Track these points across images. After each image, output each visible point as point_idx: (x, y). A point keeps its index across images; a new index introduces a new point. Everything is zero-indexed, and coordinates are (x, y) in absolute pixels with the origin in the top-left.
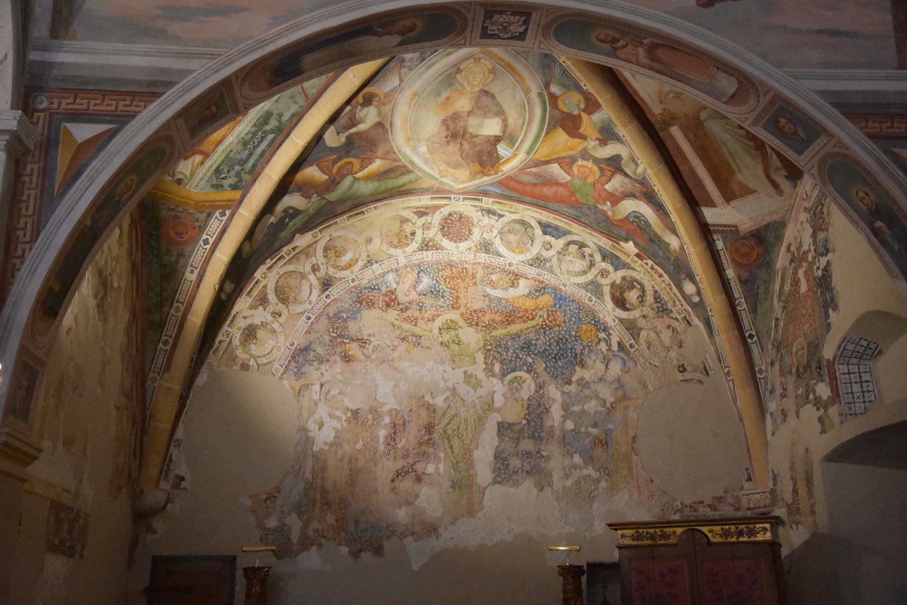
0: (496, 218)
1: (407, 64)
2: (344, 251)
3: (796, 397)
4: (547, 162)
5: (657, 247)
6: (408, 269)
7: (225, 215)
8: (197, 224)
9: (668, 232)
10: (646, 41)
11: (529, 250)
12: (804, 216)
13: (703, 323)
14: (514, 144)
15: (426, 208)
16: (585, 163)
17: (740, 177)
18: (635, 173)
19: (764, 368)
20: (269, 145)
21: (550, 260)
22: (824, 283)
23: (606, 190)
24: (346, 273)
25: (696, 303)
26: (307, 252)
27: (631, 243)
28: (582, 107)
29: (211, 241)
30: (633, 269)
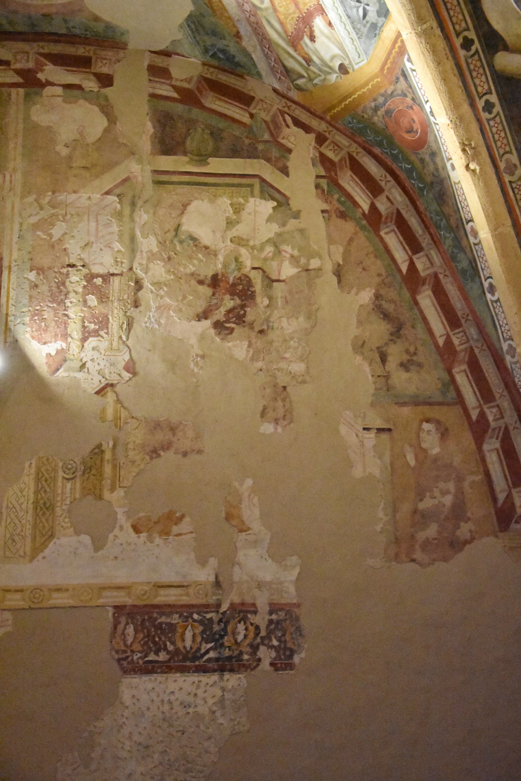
8: (409, 100)
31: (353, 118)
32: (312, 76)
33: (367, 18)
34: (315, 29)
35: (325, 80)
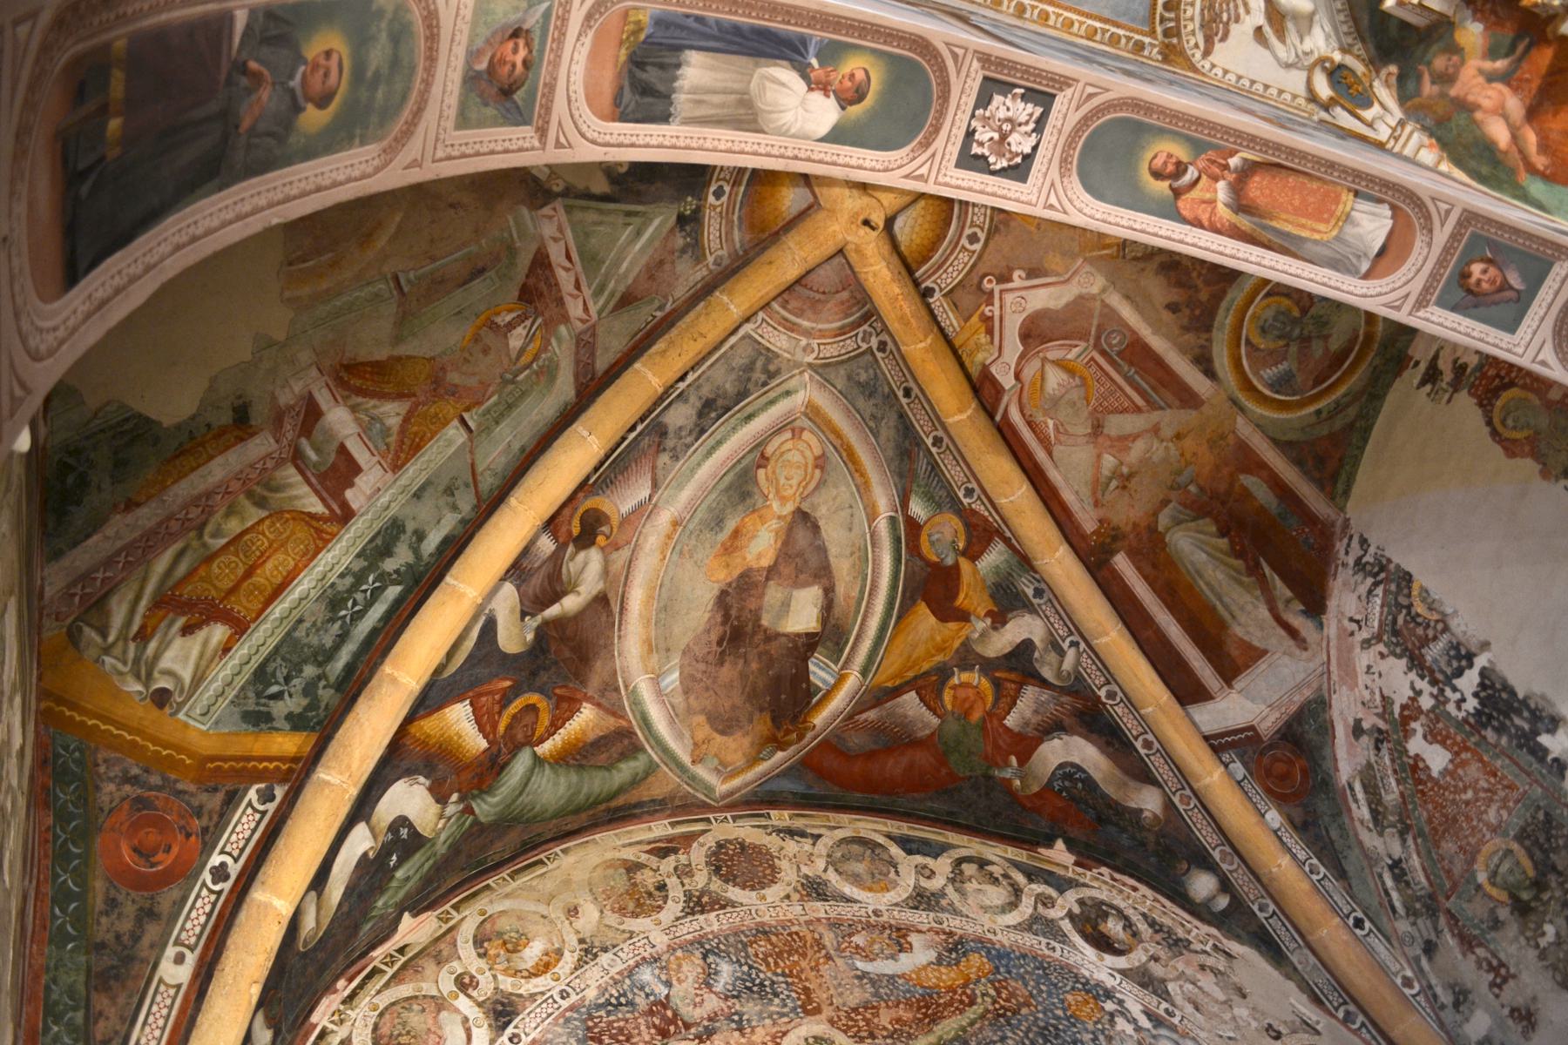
0: (810, 841)
1: (670, 443)
3: (1543, 955)
4: (896, 692)
5: (1112, 829)
6: (679, 953)
7: (272, 798)
8: (197, 824)
9: (1132, 783)
10: (1234, 162)
11: (895, 884)
12: (1363, 659)
13: (1251, 944)
14: (842, 651)
16: (965, 677)
17: (1238, 631)
19: (1409, 973)
20: (387, 617)
21: (942, 894)
22: (1498, 700)
23: (1007, 729)
25: (1224, 913)
26: (438, 950)
27: (1060, 844)
28: (961, 545)
29: (234, 869)
31: (77, 749)
32: (117, 651)
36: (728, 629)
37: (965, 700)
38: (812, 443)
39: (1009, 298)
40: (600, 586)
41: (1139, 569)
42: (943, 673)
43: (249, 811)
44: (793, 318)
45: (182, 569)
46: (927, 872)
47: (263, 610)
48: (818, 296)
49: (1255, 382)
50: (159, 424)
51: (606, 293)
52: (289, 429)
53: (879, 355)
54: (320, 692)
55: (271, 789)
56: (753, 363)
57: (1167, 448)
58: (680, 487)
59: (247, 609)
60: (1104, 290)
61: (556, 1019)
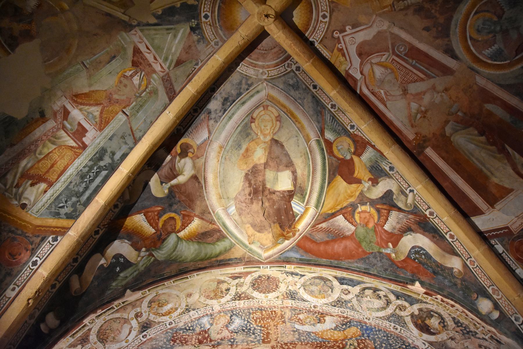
0: (299, 277)
1: (213, 116)
2: (167, 302)
4: (334, 215)
5: (440, 278)
6: (222, 314)
8: (31, 247)
9: (447, 255)
14: (304, 197)
15: (240, 274)
16: (363, 208)
17: (495, 180)
18: (406, 204)
23: (386, 231)
24: (166, 318)
25: (496, 320)
26: (133, 305)
27: (417, 284)
28: (353, 150)
30: (426, 303)
33: (60, 209)
34: (38, 185)
35: (11, 198)
36: (252, 189)
37: (365, 218)
38: (274, 111)
39: (347, 39)
40: (193, 172)
41: (439, 154)
42: (354, 207)
43: (48, 244)
44: (254, 62)
45: (29, 165)
46: (347, 292)
47: (58, 179)
48: (263, 52)
49: (481, 57)
50: (17, 118)
51: (169, 61)
52: (60, 117)
53: (297, 72)
54: (78, 206)
55: (57, 237)
56: (241, 81)
57: (441, 96)
58: (220, 133)
59: (52, 178)
60: (389, 27)
61: (163, 332)
